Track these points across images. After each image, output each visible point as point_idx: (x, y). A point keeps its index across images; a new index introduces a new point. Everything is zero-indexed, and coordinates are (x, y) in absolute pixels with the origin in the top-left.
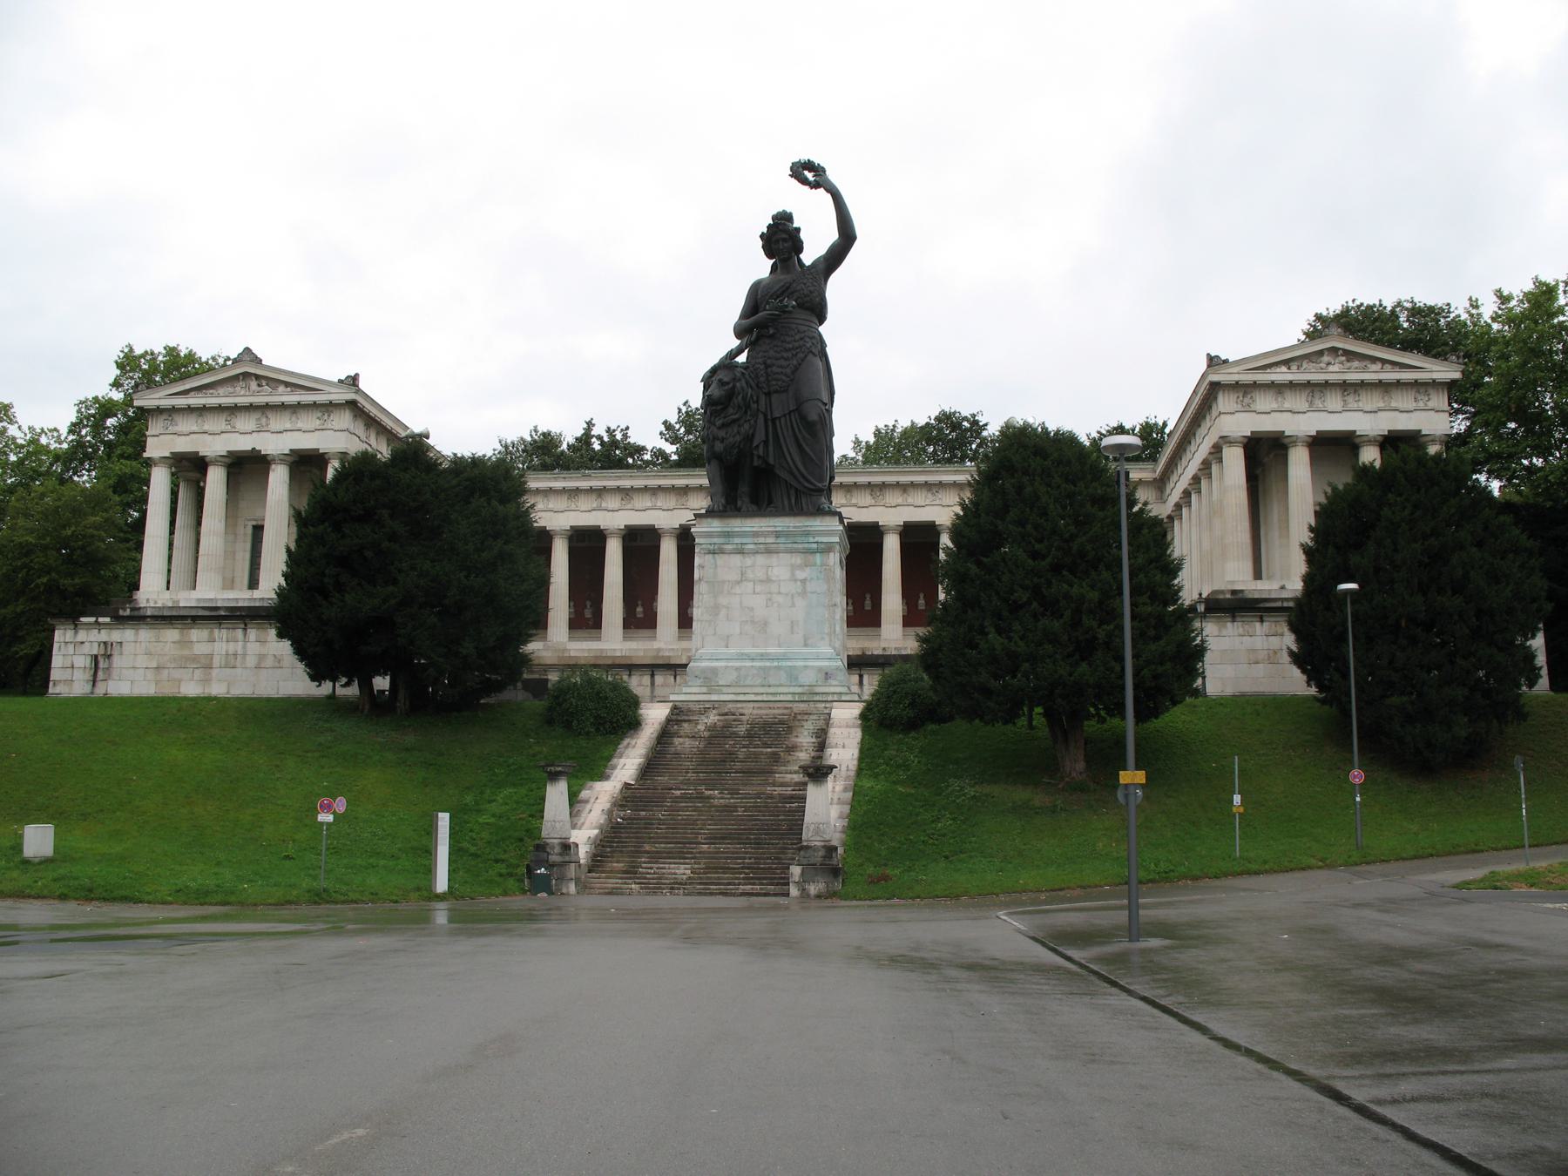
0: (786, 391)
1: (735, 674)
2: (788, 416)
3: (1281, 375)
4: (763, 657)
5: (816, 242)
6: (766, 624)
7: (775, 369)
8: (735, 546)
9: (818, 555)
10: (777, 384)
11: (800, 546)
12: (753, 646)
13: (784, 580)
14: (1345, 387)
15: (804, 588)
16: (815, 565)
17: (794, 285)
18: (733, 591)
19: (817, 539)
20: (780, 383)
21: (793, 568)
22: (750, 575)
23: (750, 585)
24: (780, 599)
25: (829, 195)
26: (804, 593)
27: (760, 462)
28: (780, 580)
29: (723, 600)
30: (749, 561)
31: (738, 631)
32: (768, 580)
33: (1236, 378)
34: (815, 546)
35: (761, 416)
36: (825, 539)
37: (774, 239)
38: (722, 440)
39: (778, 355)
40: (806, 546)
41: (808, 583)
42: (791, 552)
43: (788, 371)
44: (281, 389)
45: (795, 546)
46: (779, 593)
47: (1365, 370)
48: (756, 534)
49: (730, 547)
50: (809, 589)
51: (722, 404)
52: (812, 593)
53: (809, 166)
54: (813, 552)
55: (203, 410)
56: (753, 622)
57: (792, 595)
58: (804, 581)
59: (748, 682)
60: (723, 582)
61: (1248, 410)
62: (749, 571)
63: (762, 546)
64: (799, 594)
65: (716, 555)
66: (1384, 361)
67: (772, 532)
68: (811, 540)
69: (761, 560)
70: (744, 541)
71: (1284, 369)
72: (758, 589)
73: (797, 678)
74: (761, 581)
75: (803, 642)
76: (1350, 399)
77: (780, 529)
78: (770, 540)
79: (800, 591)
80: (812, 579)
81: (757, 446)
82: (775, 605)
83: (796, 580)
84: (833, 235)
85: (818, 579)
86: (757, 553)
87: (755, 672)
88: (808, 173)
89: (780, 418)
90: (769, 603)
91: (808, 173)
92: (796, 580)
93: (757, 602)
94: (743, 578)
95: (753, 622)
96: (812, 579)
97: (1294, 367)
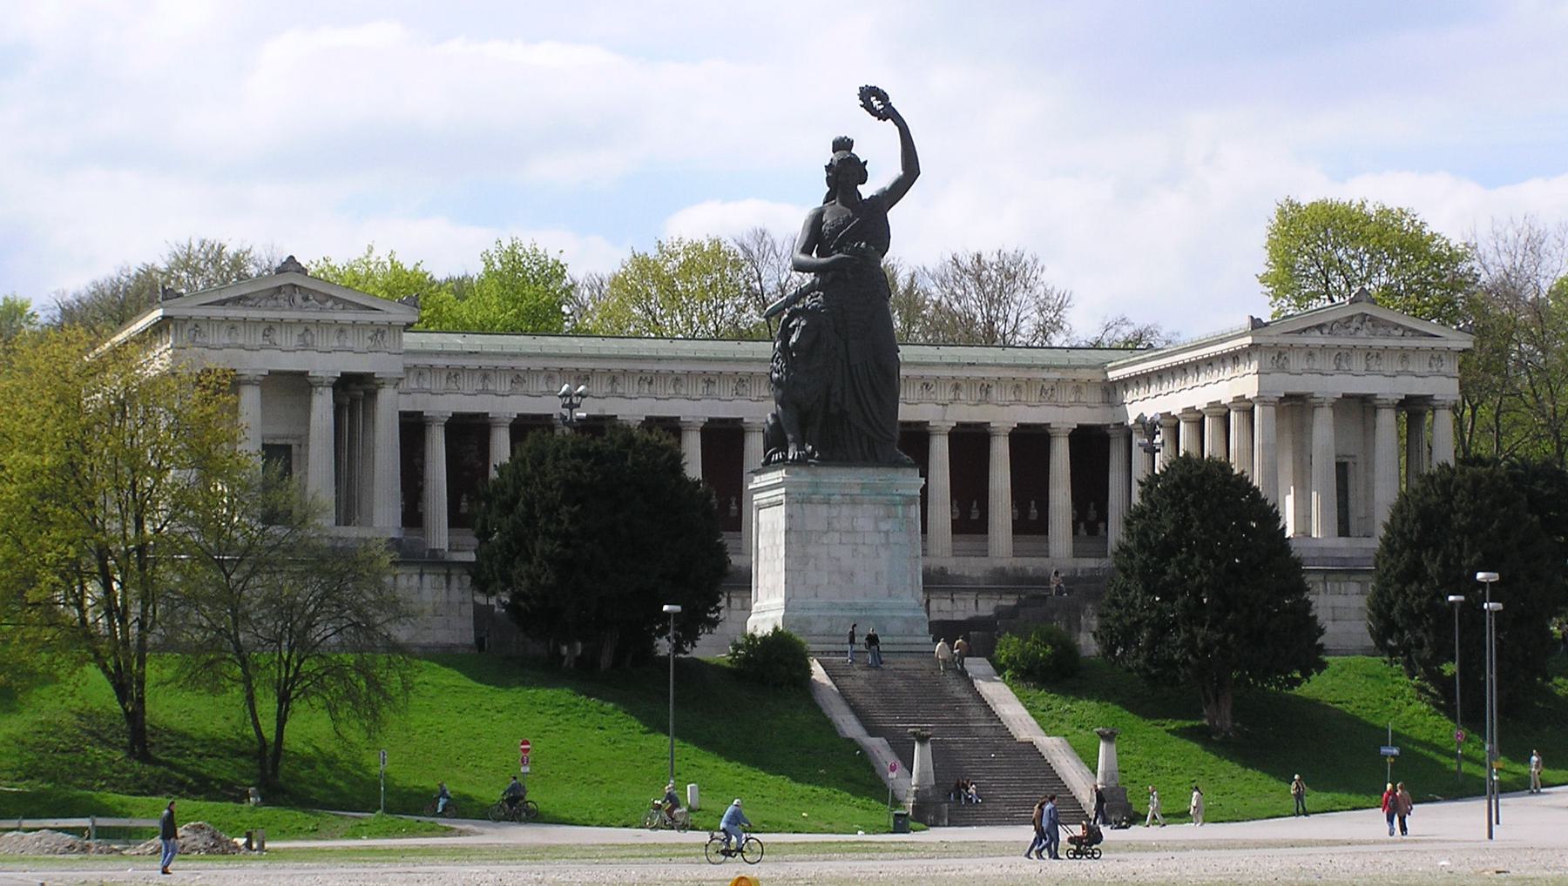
3: (1315, 339)
5: (881, 174)
14: (1371, 354)
16: (897, 517)
19: (899, 492)
21: (877, 520)
22: (836, 525)
23: (837, 535)
25: (897, 128)
26: (887, 545)
29: (811, 550)
32: (853, 531)
33: (1275, 340)
36: (907, 492)
40: (889, 498)
41: (891, 535)
45: (879, 497)
46: (864, 544)
47: (1389, 335)
50: (891, 540)
52: (896, 544)
55: (232, 325)
57: (877, 546)
58: (887, 533)
60: (811, 531)
61: (1282, 369)
62: (835, 521)
63: (848, 497)
64: (883, 545)
65: (804, 505)
66: (1406, 329)
69: (846, 510)
71: (1318, 333)
76: (1374, 366)
79: (883, 541)
84: (897, 171)
85: (900, 530)
88: (875, 101)
91: (875, 101)
92: (879, 532)
94: (830, 529)
97: (1326, 331)
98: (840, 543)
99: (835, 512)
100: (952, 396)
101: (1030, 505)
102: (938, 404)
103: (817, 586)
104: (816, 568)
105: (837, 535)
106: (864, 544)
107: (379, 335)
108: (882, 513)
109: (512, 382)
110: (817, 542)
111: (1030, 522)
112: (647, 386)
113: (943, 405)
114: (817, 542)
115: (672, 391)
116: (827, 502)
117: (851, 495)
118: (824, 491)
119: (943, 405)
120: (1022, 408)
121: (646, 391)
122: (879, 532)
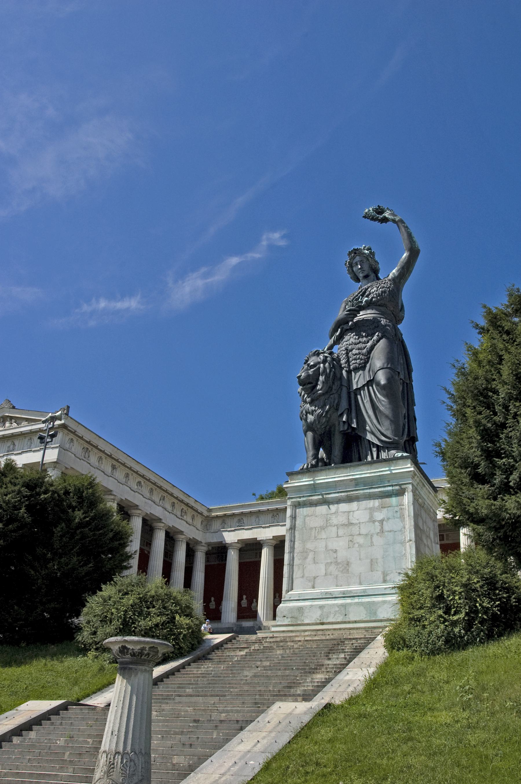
0: (363, 368)
1: (319, 613)
2: (366, 388)
4: (345, 596)
6: (348, 564)
7: (354, 351)
10: (356, 363)
12: (337, 586)
13: (363, 523)
15: (382, 528)
17: (369, 290)
18: (319, 537)
20: (358, 361)
21: (372, 510)
22: (335, 520)
23: (334, 529)
24: (360, 540)
27: (346, 428)
28: (360, 523)
29: (310, 545)
30: (333, 508)
31: (323, 572)
32: (350, 524)
35: (345, 390)
37: (354, 262)
38: (312, 413)
39: (357, 341)
41: (385, 523)
43: (364, 351)
44: (24, 423)
46: (360, 534)
51: (310, 383)
52: (390, 531)
53: (380, 211)
56: (337, 563)
58: (382, 522)
59: (330, 620)
60: (311, 529)
69: (343, 507)
72: (341, 532)
73: (375, 614)
74: (343, 525)
82: (357, 545)
87: (337, 609)
89: (359, 389)
90: (351, 545)
92: (374, 522)
93: (340, 544)
95: (337, 563)
96: (388, 519)
98: (338, 536)
103: (315, 578)
104: (315, 562)
105: (334, 529)
106: (360, 534)
110: (315, 537)
122: (374, 522)
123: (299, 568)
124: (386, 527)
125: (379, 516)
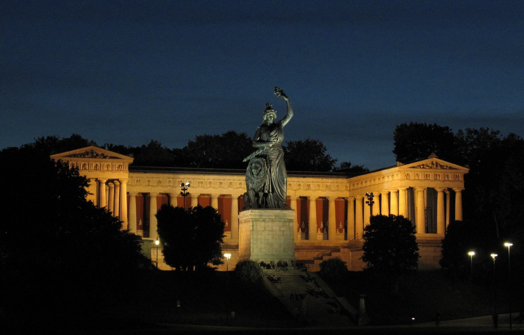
8: (263, 220)
9: (287, 223)
11: (282, 220)
16: (287, 226)
19: (287, 218)
21: (280, 227)
22: (267, 229)
23: (267, 232)
32: (272, 231)
34: (287, 220)
40: (284, 220)
42: (279, 221)
45: (281, 220)
46: (276, 235)
48: (269, 216)
49: (261, 220)
54: (285, 222)
58: (283, 231)
60: (259, 231)
67: (274, 215)
68: (286, 218)
69: (270, 224)
70: (265, 217)
75: (283, 250)
77: (277, 214)
78: (274, 217)
80: (286, 231)
81: (267, 186)
83: (281, 231)
85: (287, 230)
86: (269, 221)
92: (281, 231)
99: (267, 225)
100: (298, 188)
101: (340, 224)
102: (293, 190)
105: (267, 232)
107: (120, 167)
108: (282, 225)
109: (158, 182)
110: (261, 234)
111: (325, 229)
112: (201, 184)
113: (295, 190)
114: (261, 234)
115: (208, 186)
116: (264, 221)
117: (272, 219)
118: (263, 217)
119: (295, 190)
120: (320, 192)
121: (200, 186)
123: (255, 245)
124: (285, 233)
125: (282, 229)
